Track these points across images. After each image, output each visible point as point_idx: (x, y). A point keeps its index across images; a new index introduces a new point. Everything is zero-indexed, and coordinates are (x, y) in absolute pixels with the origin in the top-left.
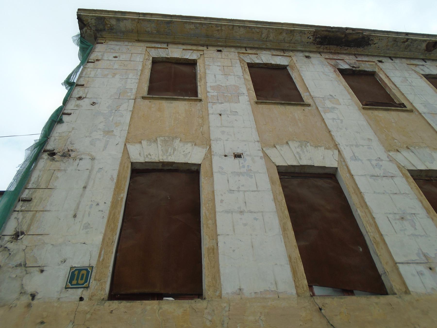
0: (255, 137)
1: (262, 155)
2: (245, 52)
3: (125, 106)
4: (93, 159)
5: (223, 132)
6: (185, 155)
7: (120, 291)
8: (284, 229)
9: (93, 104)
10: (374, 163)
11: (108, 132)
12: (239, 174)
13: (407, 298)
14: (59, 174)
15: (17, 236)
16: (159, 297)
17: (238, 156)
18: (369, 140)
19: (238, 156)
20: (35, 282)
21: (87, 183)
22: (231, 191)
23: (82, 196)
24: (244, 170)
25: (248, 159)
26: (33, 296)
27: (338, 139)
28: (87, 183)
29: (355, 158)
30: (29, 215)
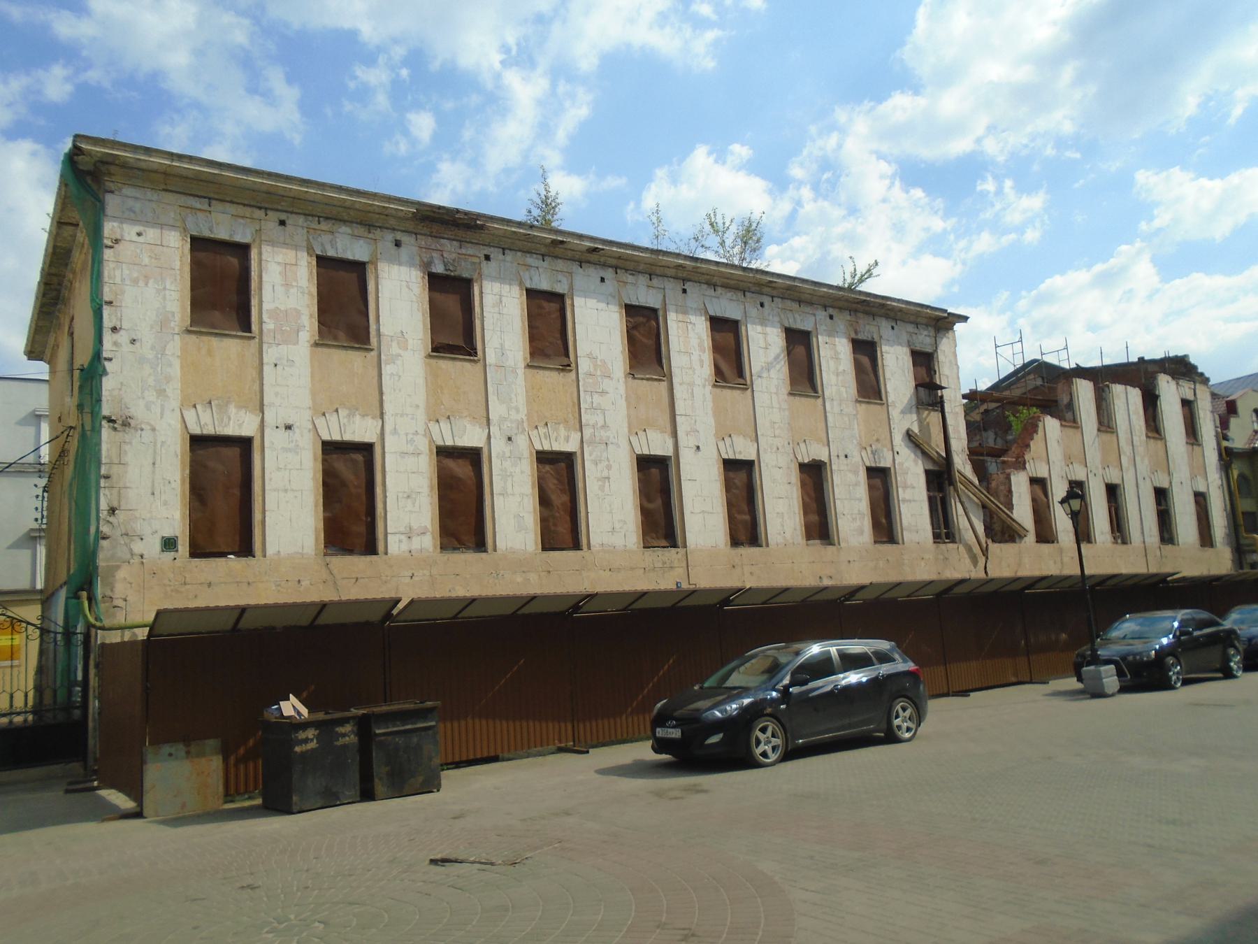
0: (308, 402)
1: (311, 427)
2: (317, 227)
3: (170, 346)
4: (154, 430)
5: (277, 394)
6: (240, 426)
7: (197, 551)
8: (316, 506)
9: (133, 341)
10: (410, 437)
11: (161, 392)
12: (286, 450)
13: (385, 557)
14: (127, 447)
15: (112, 511)
16: (223, 555)
17: (288, 427)
18: (417, 406)
19: (288, 427)
20: (138, 547)
21: (154, 458)
22: (279, 469)
23: (154, 472)
24: (292, 445)
25: (297, 431)
26: (142, 556)
27: (388, 407)
28: (154, 458)
29: (395, 431)
30: (115, 491)
